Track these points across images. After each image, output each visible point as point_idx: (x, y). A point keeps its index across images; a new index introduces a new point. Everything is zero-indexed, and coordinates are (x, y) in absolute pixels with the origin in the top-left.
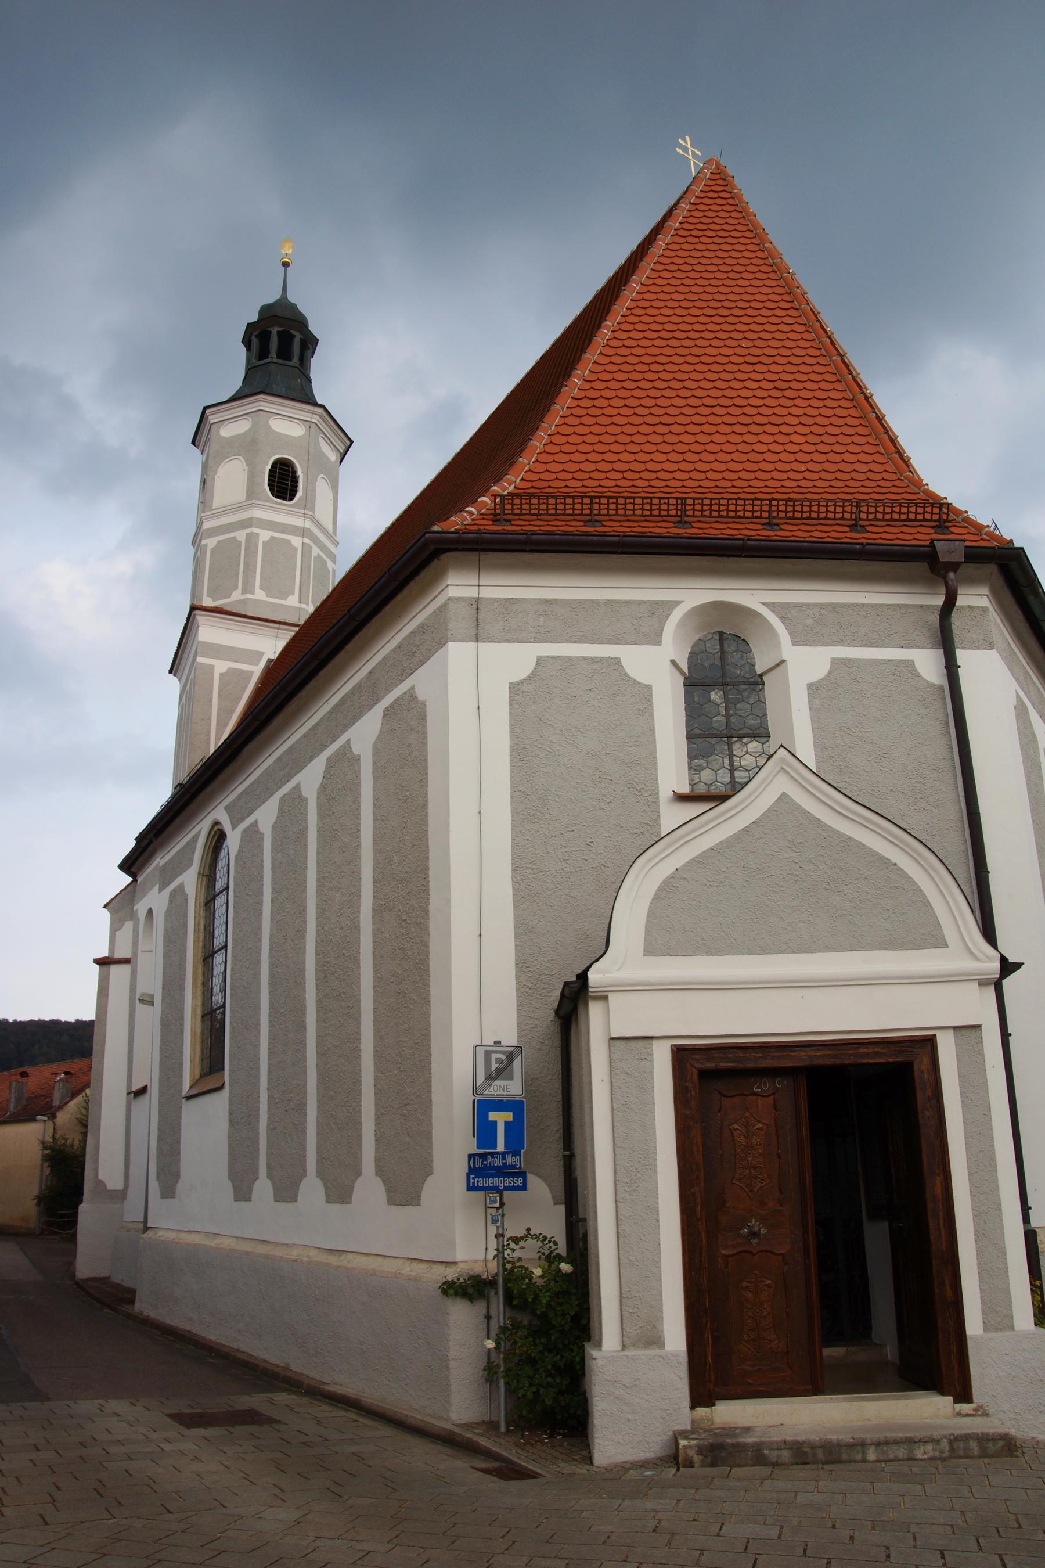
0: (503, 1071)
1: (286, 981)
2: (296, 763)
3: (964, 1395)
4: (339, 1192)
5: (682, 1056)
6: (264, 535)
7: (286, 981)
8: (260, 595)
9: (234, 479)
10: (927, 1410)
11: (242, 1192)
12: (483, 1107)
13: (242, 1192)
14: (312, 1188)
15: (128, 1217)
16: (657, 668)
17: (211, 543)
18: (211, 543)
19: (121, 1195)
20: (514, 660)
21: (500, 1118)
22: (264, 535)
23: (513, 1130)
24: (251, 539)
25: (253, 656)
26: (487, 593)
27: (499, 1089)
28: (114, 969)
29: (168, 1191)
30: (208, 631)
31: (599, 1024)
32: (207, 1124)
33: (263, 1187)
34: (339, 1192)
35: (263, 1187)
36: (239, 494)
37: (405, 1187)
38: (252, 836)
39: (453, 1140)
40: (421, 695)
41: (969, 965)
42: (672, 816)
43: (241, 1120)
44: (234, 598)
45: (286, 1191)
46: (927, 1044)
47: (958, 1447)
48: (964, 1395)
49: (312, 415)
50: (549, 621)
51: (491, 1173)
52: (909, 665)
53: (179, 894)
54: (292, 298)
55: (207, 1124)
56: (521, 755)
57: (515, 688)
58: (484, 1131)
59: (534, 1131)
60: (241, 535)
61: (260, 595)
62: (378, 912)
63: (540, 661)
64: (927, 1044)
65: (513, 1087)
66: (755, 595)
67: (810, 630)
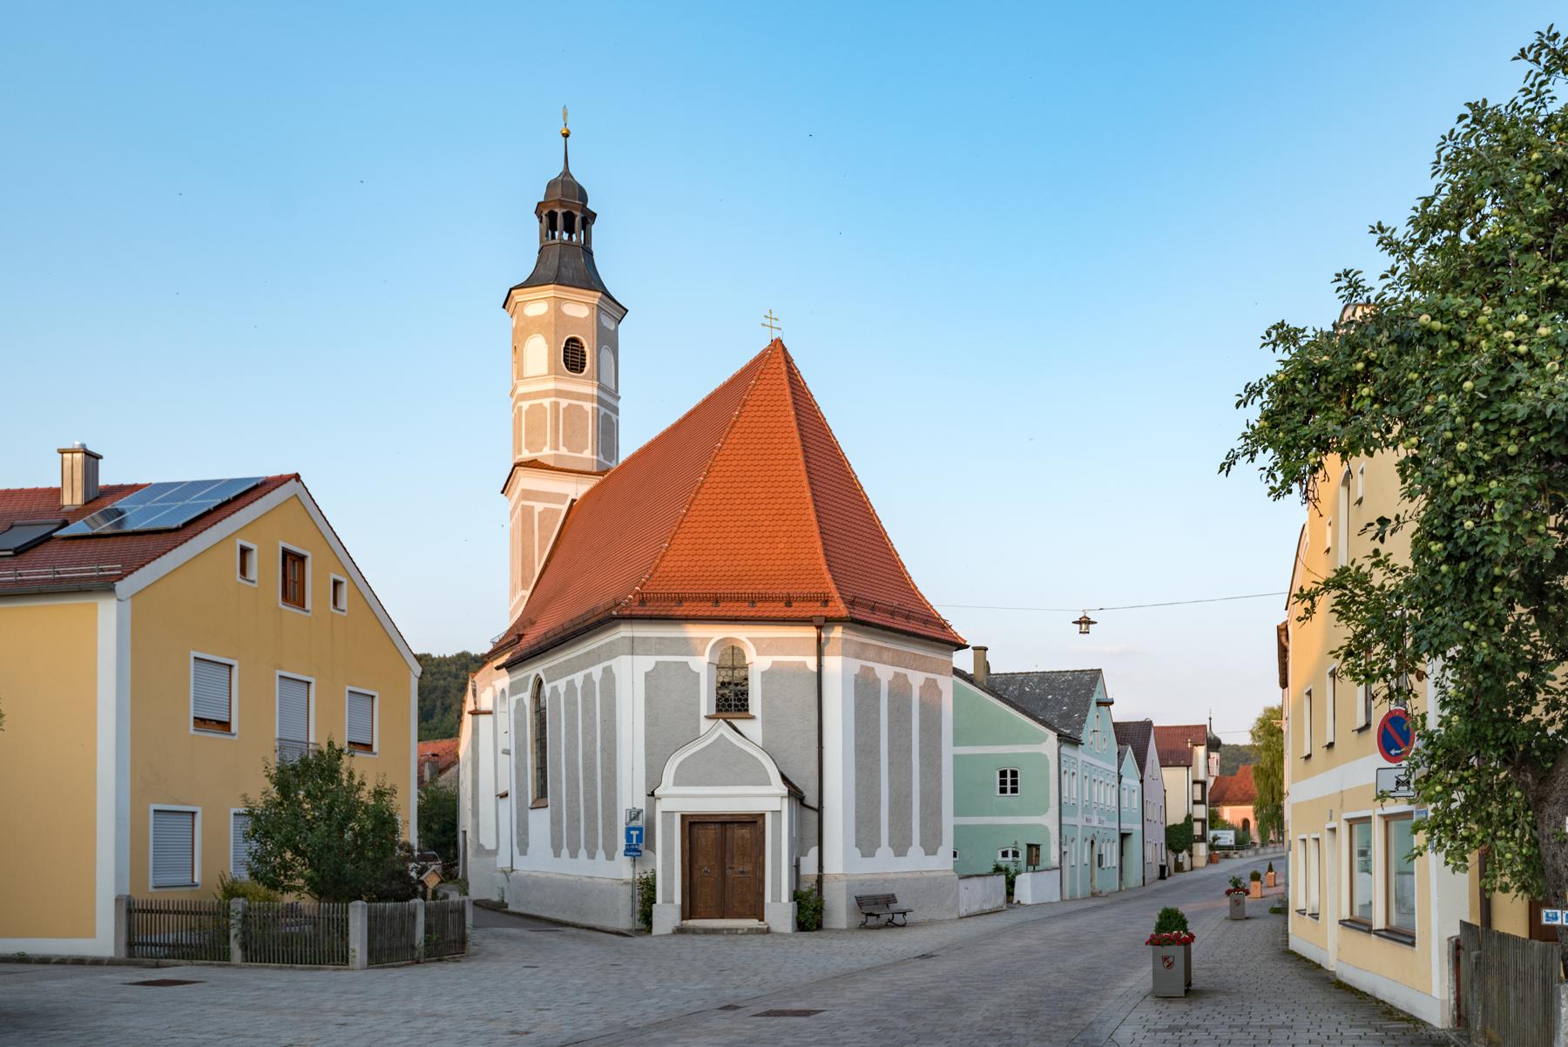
0: (636, 817)
1: (572, 765)
2: (571, 668)
3: (762, 919)
4: (592, 856)
5: (683, 817)
6: (564, 403)
7: (572, 765)
8: (563, 451)
9: (540, 353)
10: (753, 923)
11: (557, 854)
12: (628, 830)
13: (557, 854)
14: (583, 853)
15: (500, 865)
16: (701, 663)
17: (525, 405)
18: (525, 405)
19: (495, 853)
20: (647, 663)
21: (634, 833)
22: (564, 403)
23: (639, 838)
24: (556, 405)
25: (558, 498)
26: (636, 634)
27: (634, 824)
28: (481, 717)
29: (523, 852)
30: (527, 481)
31: (661, 807)
32: (540, 821)
33: (565, 852)
34: (592, 856)
35: (565, 852)
36: (544, 369)
37: (610, 856)
38: (555, 689)
39: (622, 842)
40: (615, 670)
41: (778, 791)
42: (705, 725)
43: (555, 822)
44: (545, 453)
45: (574, 854)
46: (762, 816)
47: (751, 931)
48: (762, 919)
49: (594, 297)
50: (662, 646)
51: (632, 851)
52: (804, 664)
53: (520, 702)
54: (579, 176)
55: (540, 821)
56: (649, 701)
57: (647, 674)
58: (629, 837)
59: (639, 841)
60: (547, 402)
61: (563, 451)
62: (603, 750)
63: (657, 663)
64: (762, 816)
65: (640, 823)
66: (742, 634)
67: (763, 647)
